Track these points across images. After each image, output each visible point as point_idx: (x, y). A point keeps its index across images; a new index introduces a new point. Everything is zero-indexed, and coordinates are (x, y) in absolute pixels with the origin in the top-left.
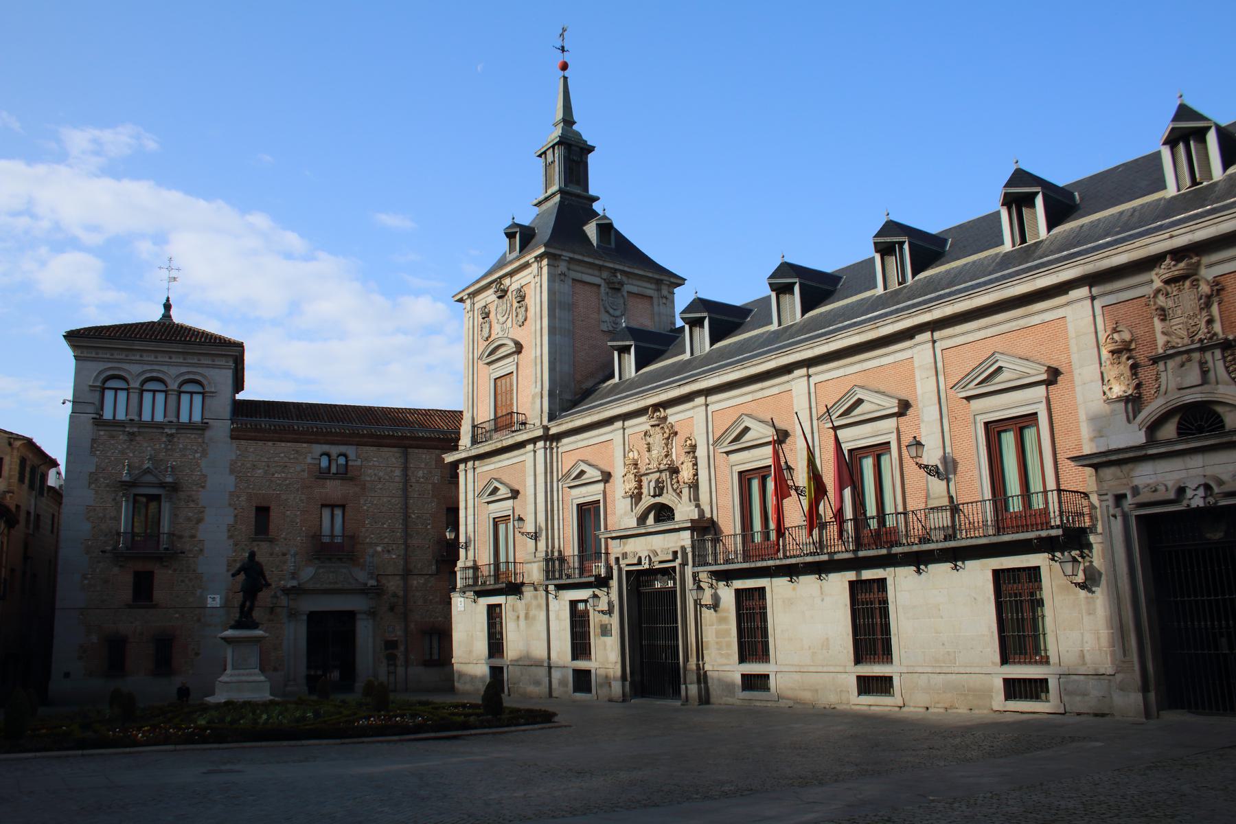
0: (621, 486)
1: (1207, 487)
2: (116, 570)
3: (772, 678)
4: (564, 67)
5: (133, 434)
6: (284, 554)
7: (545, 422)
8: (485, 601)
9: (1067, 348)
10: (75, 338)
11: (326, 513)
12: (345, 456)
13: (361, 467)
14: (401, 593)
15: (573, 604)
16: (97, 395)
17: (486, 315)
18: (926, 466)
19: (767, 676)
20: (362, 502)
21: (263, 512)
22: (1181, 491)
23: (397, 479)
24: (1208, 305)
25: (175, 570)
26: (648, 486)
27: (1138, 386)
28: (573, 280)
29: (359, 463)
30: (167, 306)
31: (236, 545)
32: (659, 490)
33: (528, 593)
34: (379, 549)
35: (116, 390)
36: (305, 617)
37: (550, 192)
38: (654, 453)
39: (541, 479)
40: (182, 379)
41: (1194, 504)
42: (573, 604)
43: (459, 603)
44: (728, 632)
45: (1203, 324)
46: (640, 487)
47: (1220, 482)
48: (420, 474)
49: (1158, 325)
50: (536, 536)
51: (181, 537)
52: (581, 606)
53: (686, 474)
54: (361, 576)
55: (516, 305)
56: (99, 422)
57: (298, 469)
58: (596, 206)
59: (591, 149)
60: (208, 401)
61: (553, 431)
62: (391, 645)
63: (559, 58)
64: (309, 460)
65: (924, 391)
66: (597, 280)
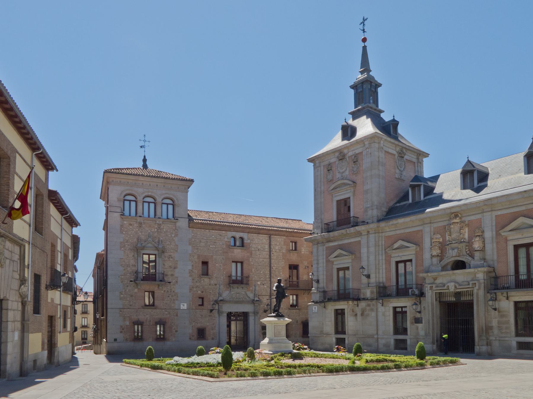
2: (136, 290)
6: (216, 285)
11: (234, 265)
13: (250, 243)
20: (251, 260)
21: (205, 263)
23: (266, 250)
25: (165, 291)
29: (249, 241)
31: (193, 280)
34: (259, 283)
44: (508, 322)
48: (277, 248)
50: (368, 276)
51: (167, 275)
54: (251, 296)
57: (221, 244)
64: (226, 240)
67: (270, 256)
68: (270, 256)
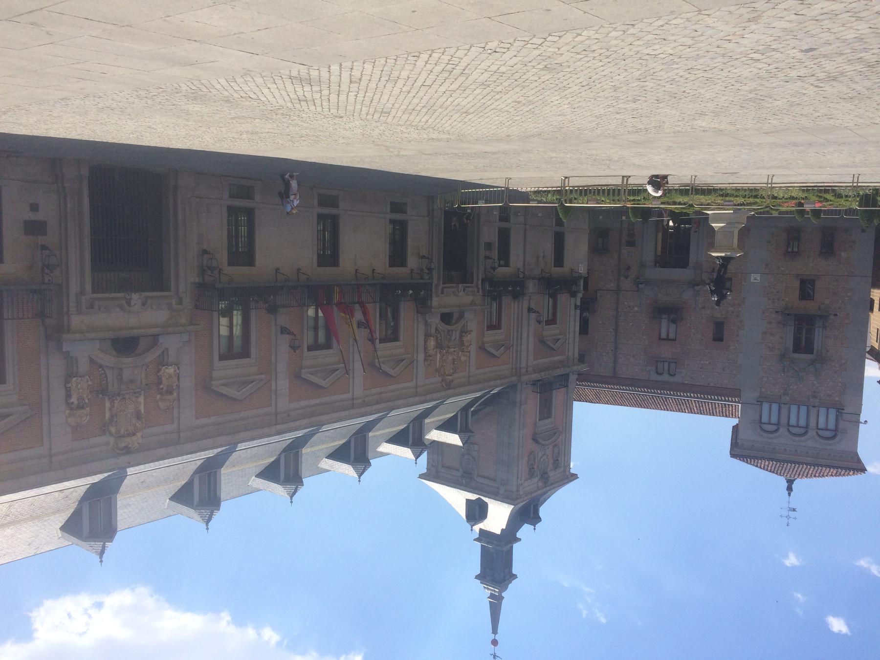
0: (471, 338)
1: (129, 304)
3: (389, 211)
5: (815, 397)
6: (703, 308)
8: (565, 270)
10: (858, 467)
11: (672, 336)
12: (658, 373)
14: (622, 278)
15: (507, 265)
16: (842, 425)
18: (289, 333)
19: (392, 211)
21: (718, 338)
22: (144, 304)
24: (112, 417)
26: (456, 336)
28: (495, 480)
30: (790, 489)
33: (537, 272)
34: (636, 309)
35: (826, 429)
36: (691, 264)
37: (509, 546)
38: (450, 358)
39: (524, 347)
40: (777, 434)
41: (138, 294)
42: (507, 265)
43: (582, 270)
45: (116, 405)
46: (461, 337)
47: (121, 307)
49: (142, 408)
51: (779, 323)
52: (502, 262)
53: (432, 343)
55: (535, 467)
56: (840, 410)
59: (477, 577)
60: (757, 418)
61: (514, 379)
62: (631, 243)
63: (498, 650)
65: (283, 383)
67: (616, 348)
68: (616, 348)
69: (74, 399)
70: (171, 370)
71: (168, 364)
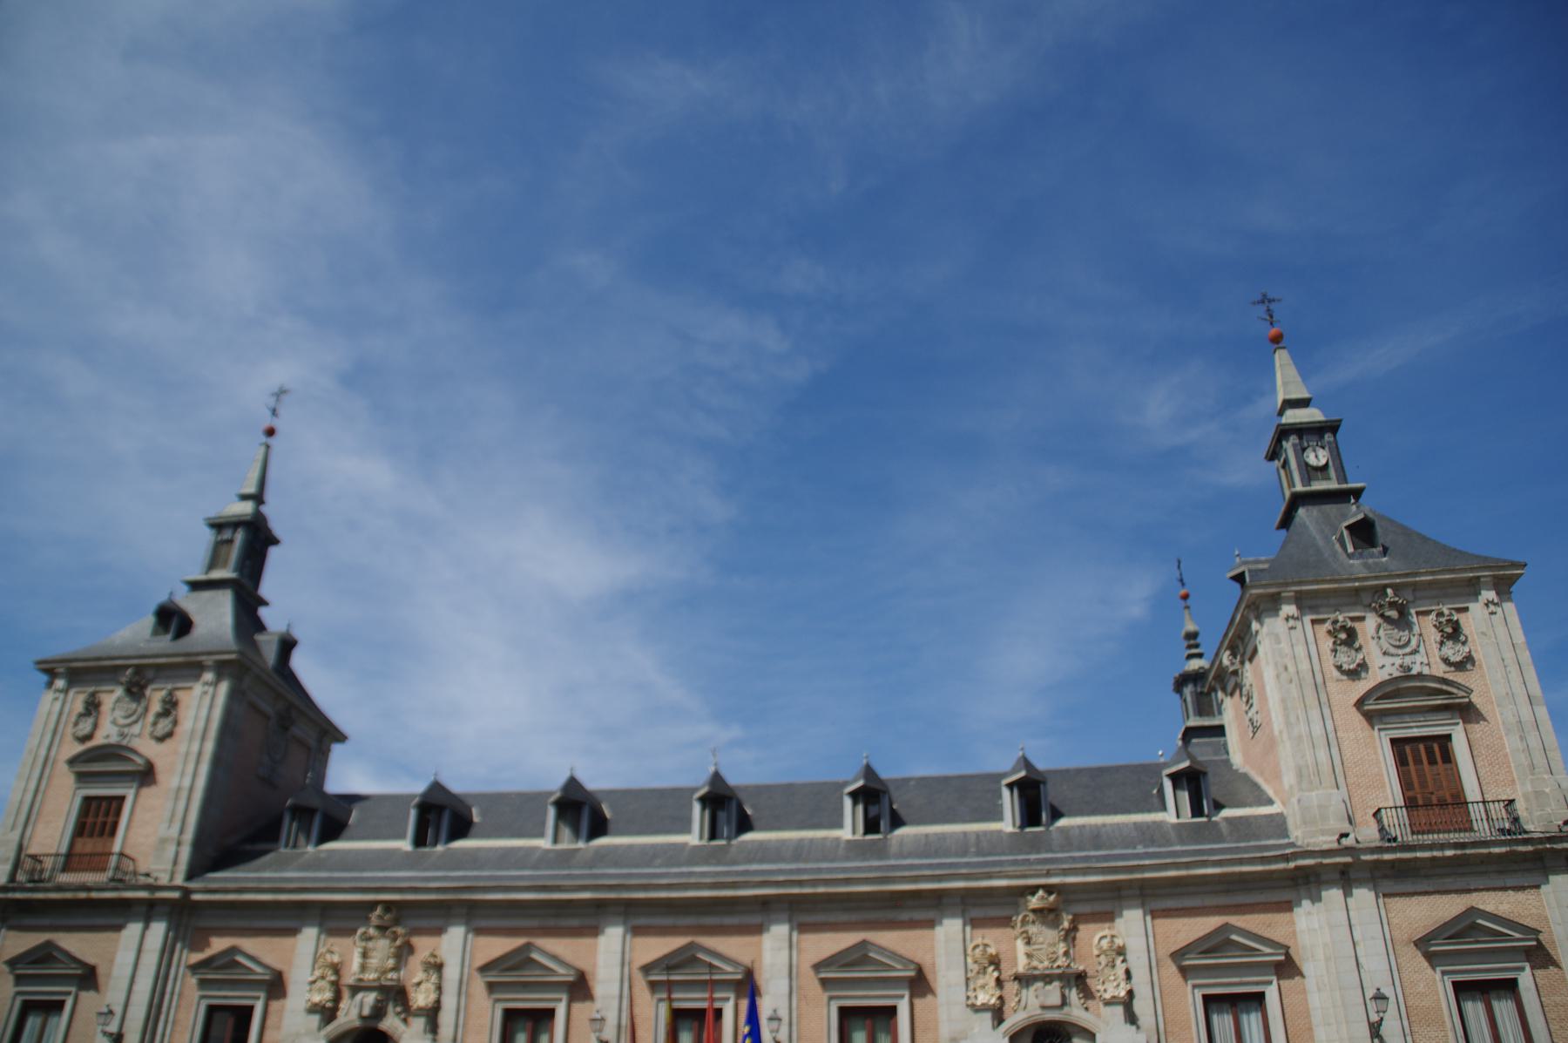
4: (270, 432)
7: (179, 880)
9: (932, 949)
17: (92, 707)
27: (1001, 998)
32: (379, 1012)
37: (217, 574)
38: (374, 962)
46: (337, 998)
49: (1020, 944)
53: (421, 998)
55: (156, 707)
58: (263, 612)
59: (275, 541)
61: (196, 897)
66: (269, 710)
69: (1120, 969)
70: (982, 998)
71: (984, 1008)
